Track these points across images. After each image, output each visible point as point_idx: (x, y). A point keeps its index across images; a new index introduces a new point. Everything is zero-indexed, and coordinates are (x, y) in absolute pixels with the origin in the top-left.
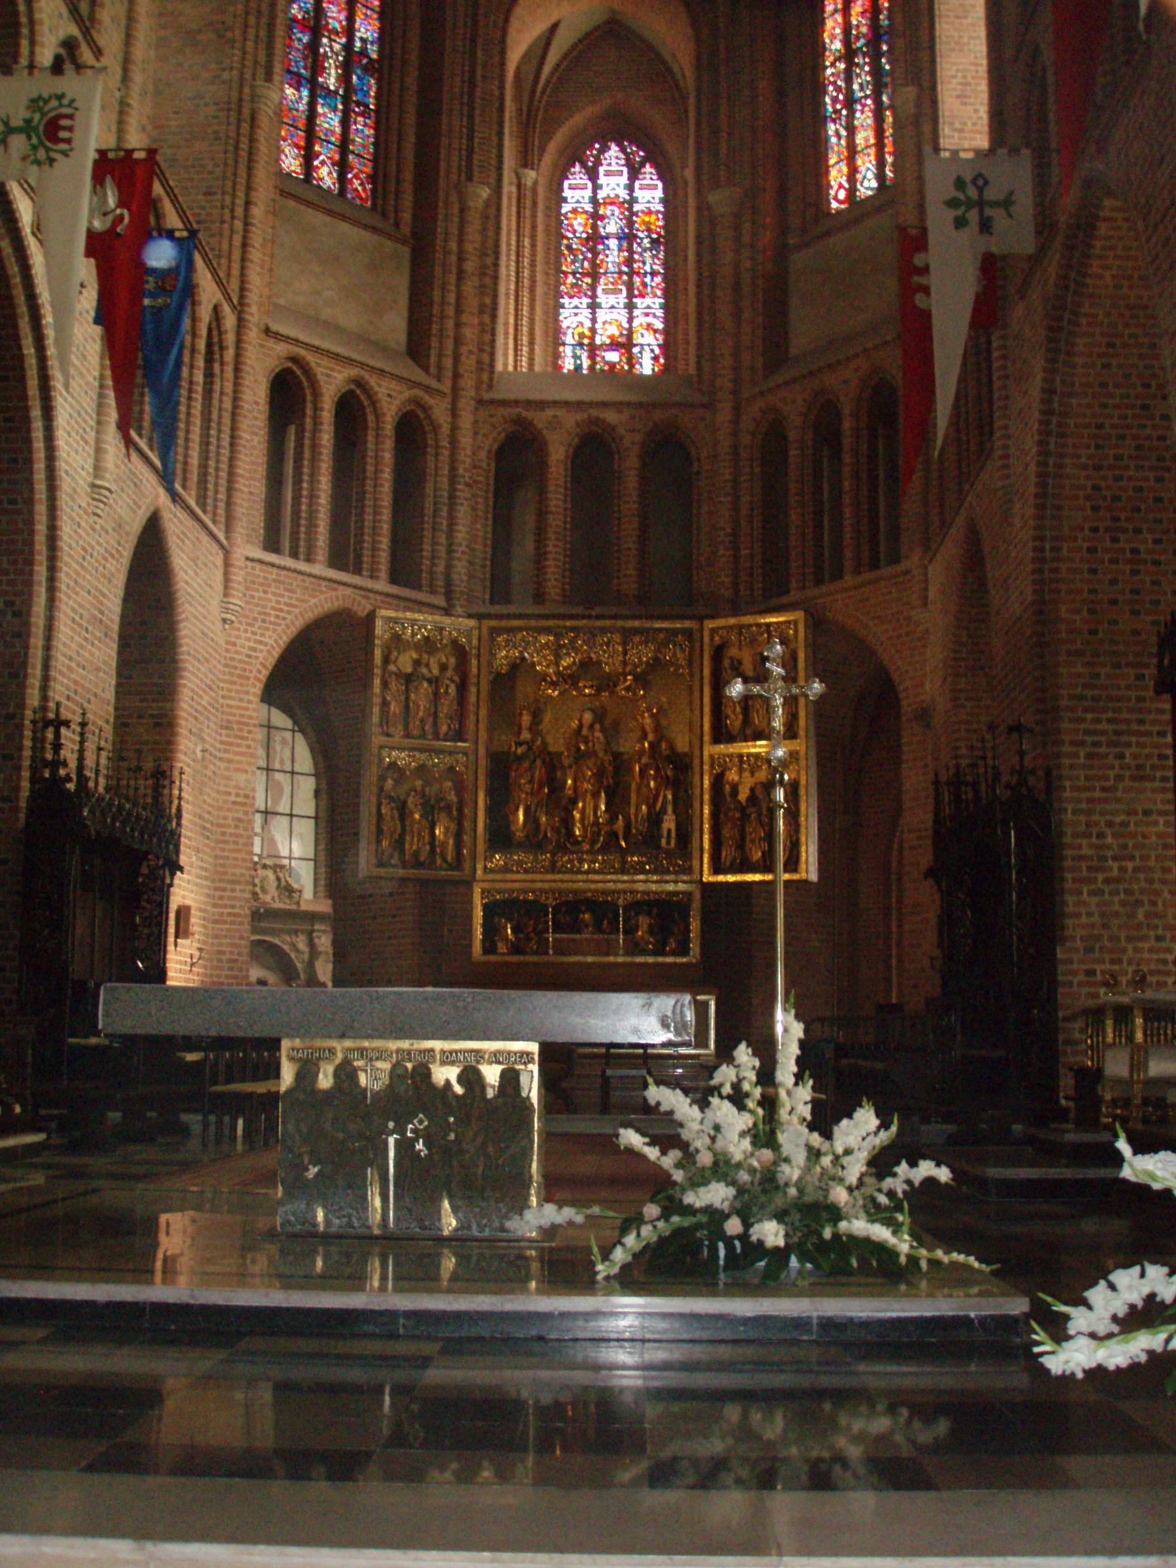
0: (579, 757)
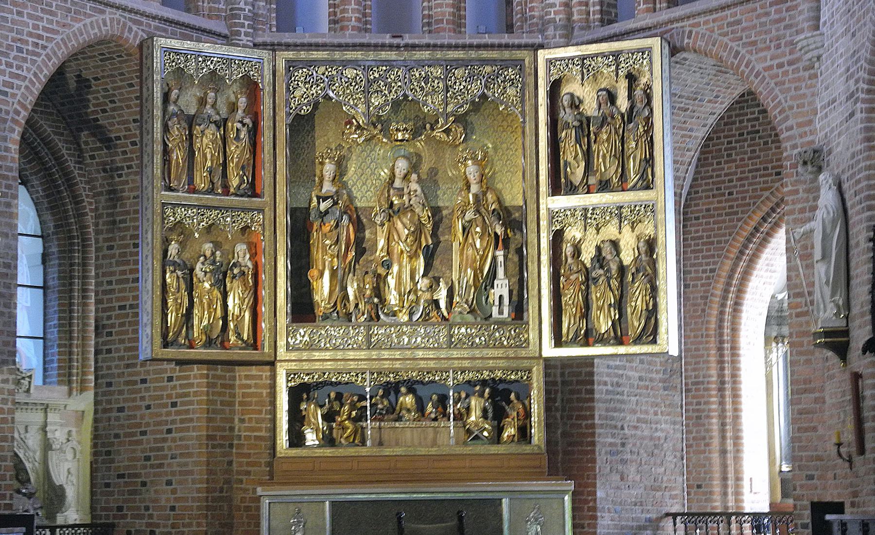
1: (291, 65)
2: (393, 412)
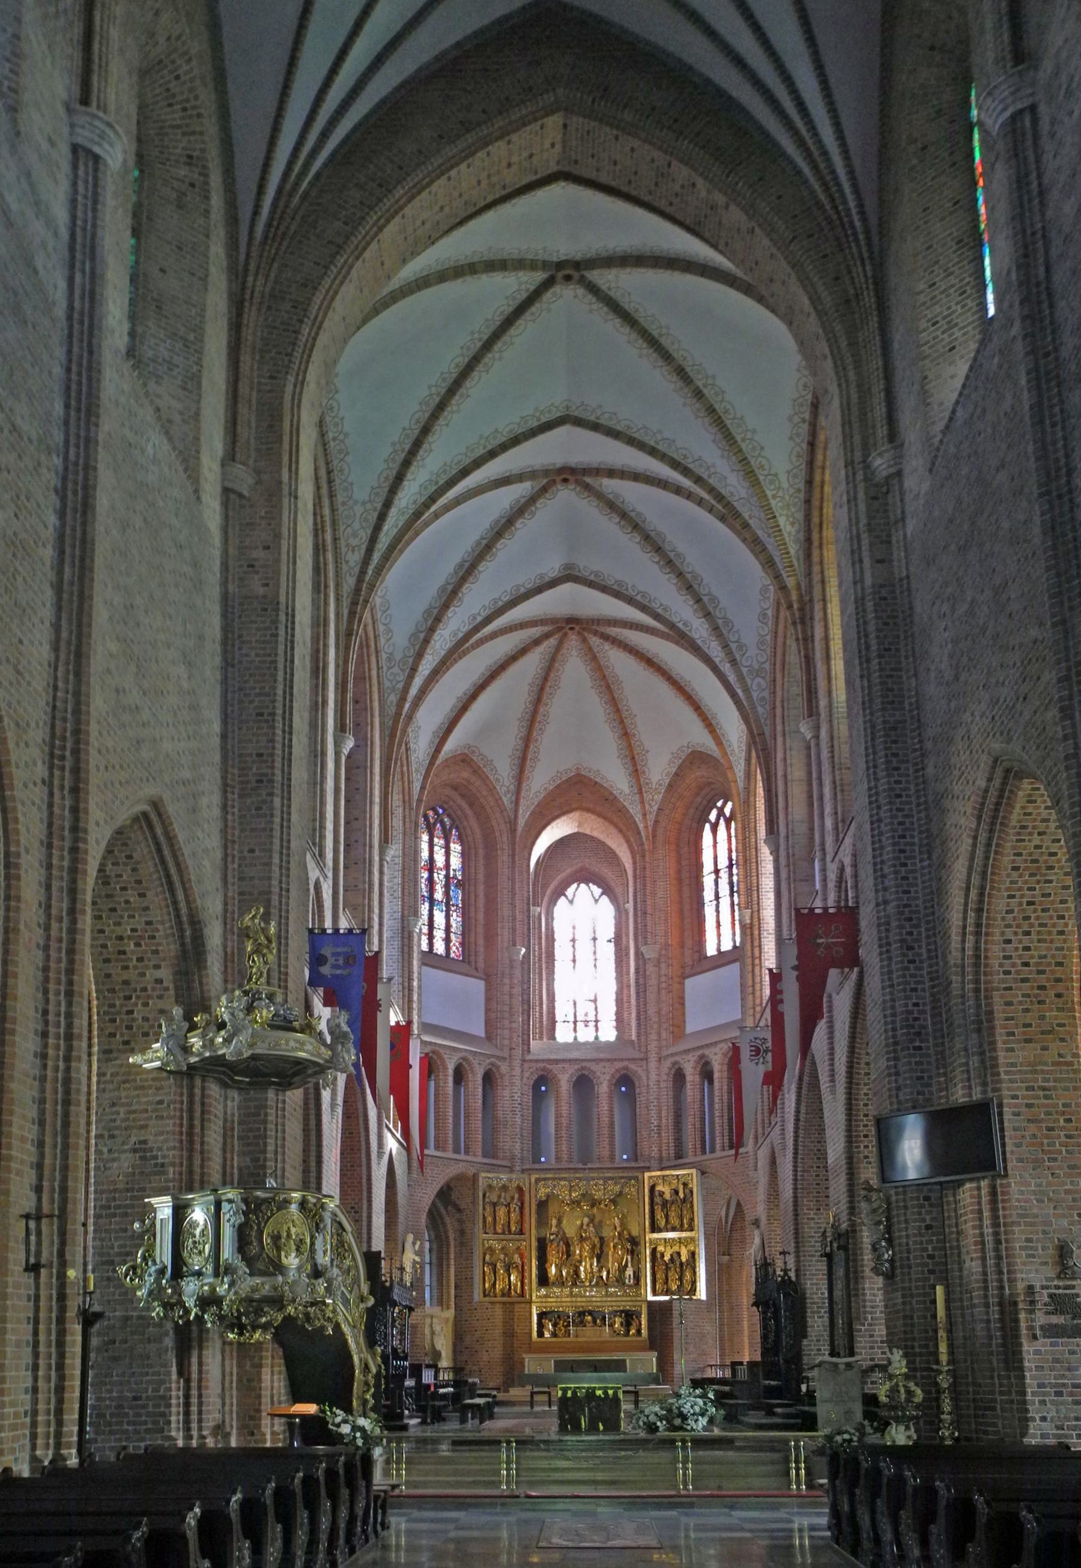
0: (582, 1239)
1: (538, 1180)
2: (582, 1323)
